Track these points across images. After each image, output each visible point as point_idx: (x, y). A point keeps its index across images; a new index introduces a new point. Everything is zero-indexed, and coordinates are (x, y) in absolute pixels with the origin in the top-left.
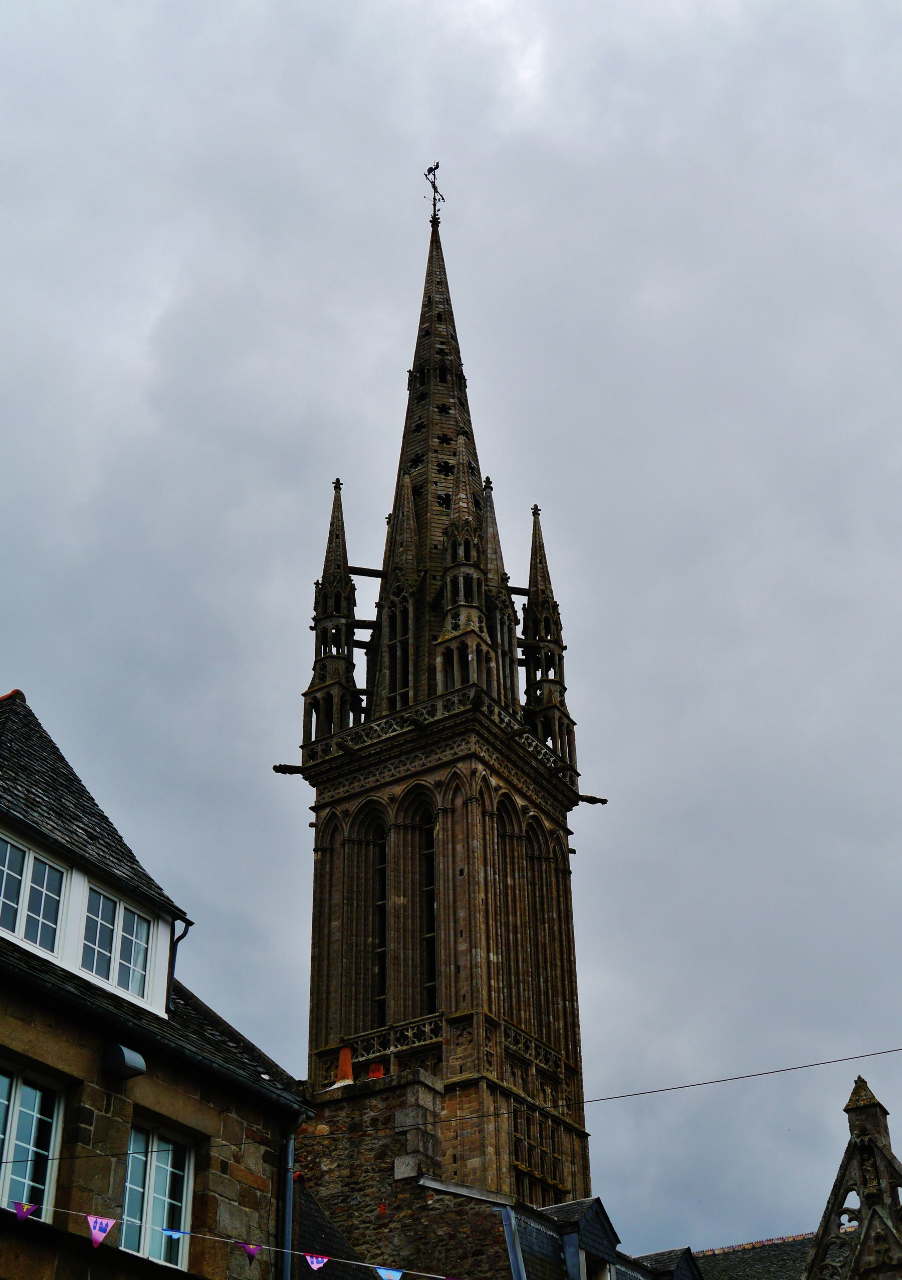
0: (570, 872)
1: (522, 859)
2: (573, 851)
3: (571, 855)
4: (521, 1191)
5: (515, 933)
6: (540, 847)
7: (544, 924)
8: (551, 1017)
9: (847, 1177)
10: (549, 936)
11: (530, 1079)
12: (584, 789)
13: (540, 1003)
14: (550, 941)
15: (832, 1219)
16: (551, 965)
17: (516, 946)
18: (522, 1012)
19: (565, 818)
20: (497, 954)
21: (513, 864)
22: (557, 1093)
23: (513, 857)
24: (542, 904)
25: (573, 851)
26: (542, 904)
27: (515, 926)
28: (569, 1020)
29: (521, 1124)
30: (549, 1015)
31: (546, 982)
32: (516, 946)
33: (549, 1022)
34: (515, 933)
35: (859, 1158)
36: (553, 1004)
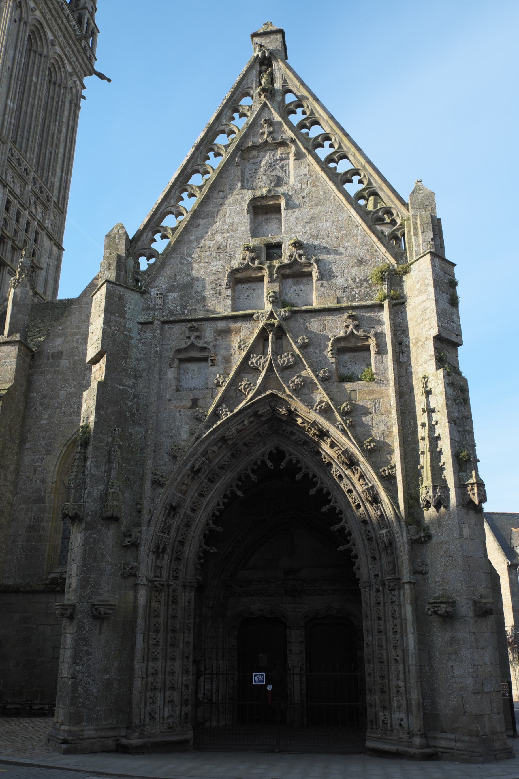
0: (80, 108)
1: (46, 70)
2: (84, 98)
3: (82, 100)
4: (5, 248)
5: (32, 109)
6: (61, 79)
7: (55, 122)
8: (50, 173)
9: (245, 82)
10: (58, 130)
11: (26, 192)
12: (97, 66)
13: (44, 164)
14: (58, 133)
15: (225, 112)
16: (56, 145)
17: (31, 116)
18: (28, 153)
19: (83, 79)
20: (14, 103)
21: (38, 70)
22: (46, 215)
23: (39, 67)
24: (57, 111)
25: (84, 98)
26: (57, 111)
27: (33, 105)
28: (63, 184)
29: (13, 210)
30: (49, 172)
31: (51, 153)
32: (31, 116)
33: (48, 175)
34: (32, 109)
35: (258, 69)
36: (53, 166)
